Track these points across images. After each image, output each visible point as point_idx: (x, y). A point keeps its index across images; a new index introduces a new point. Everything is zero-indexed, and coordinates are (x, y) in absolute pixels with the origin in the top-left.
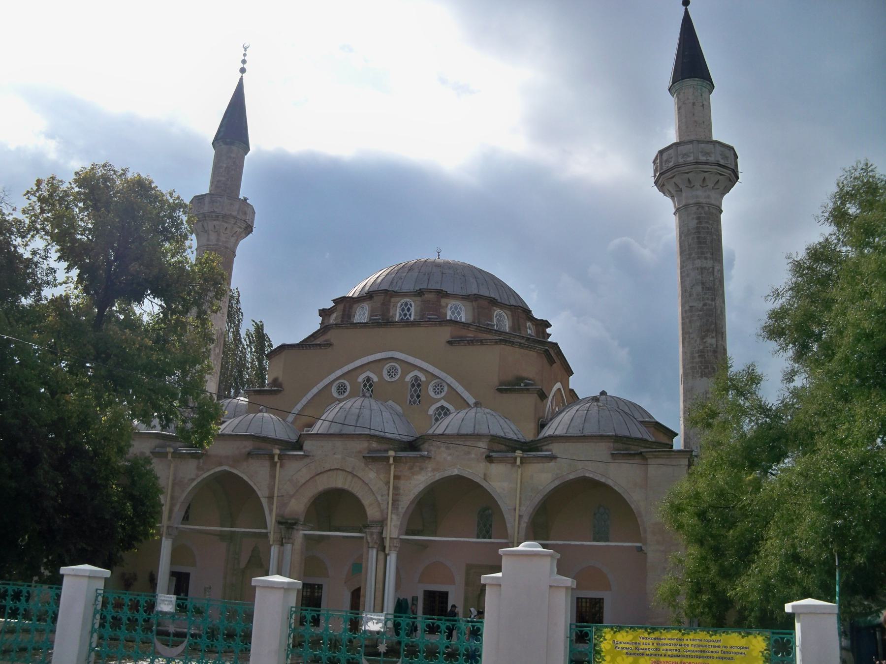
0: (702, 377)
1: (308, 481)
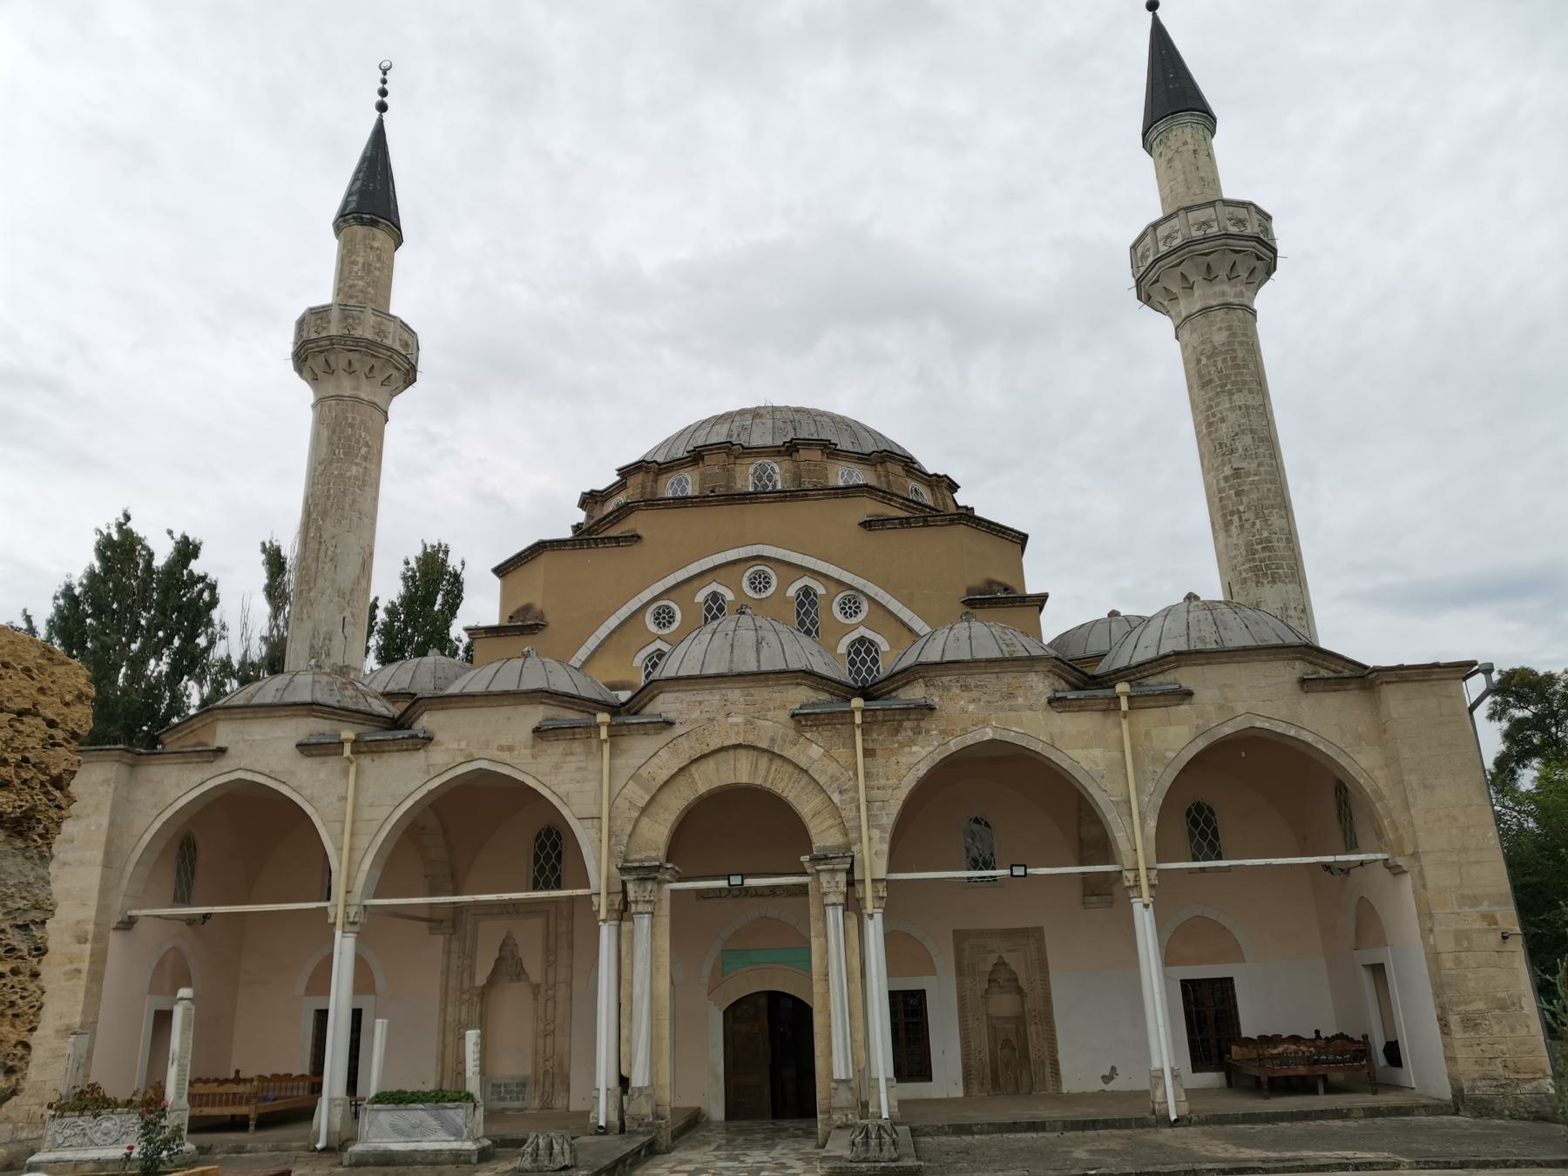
0: (1274, 581)
1: (673, 777)
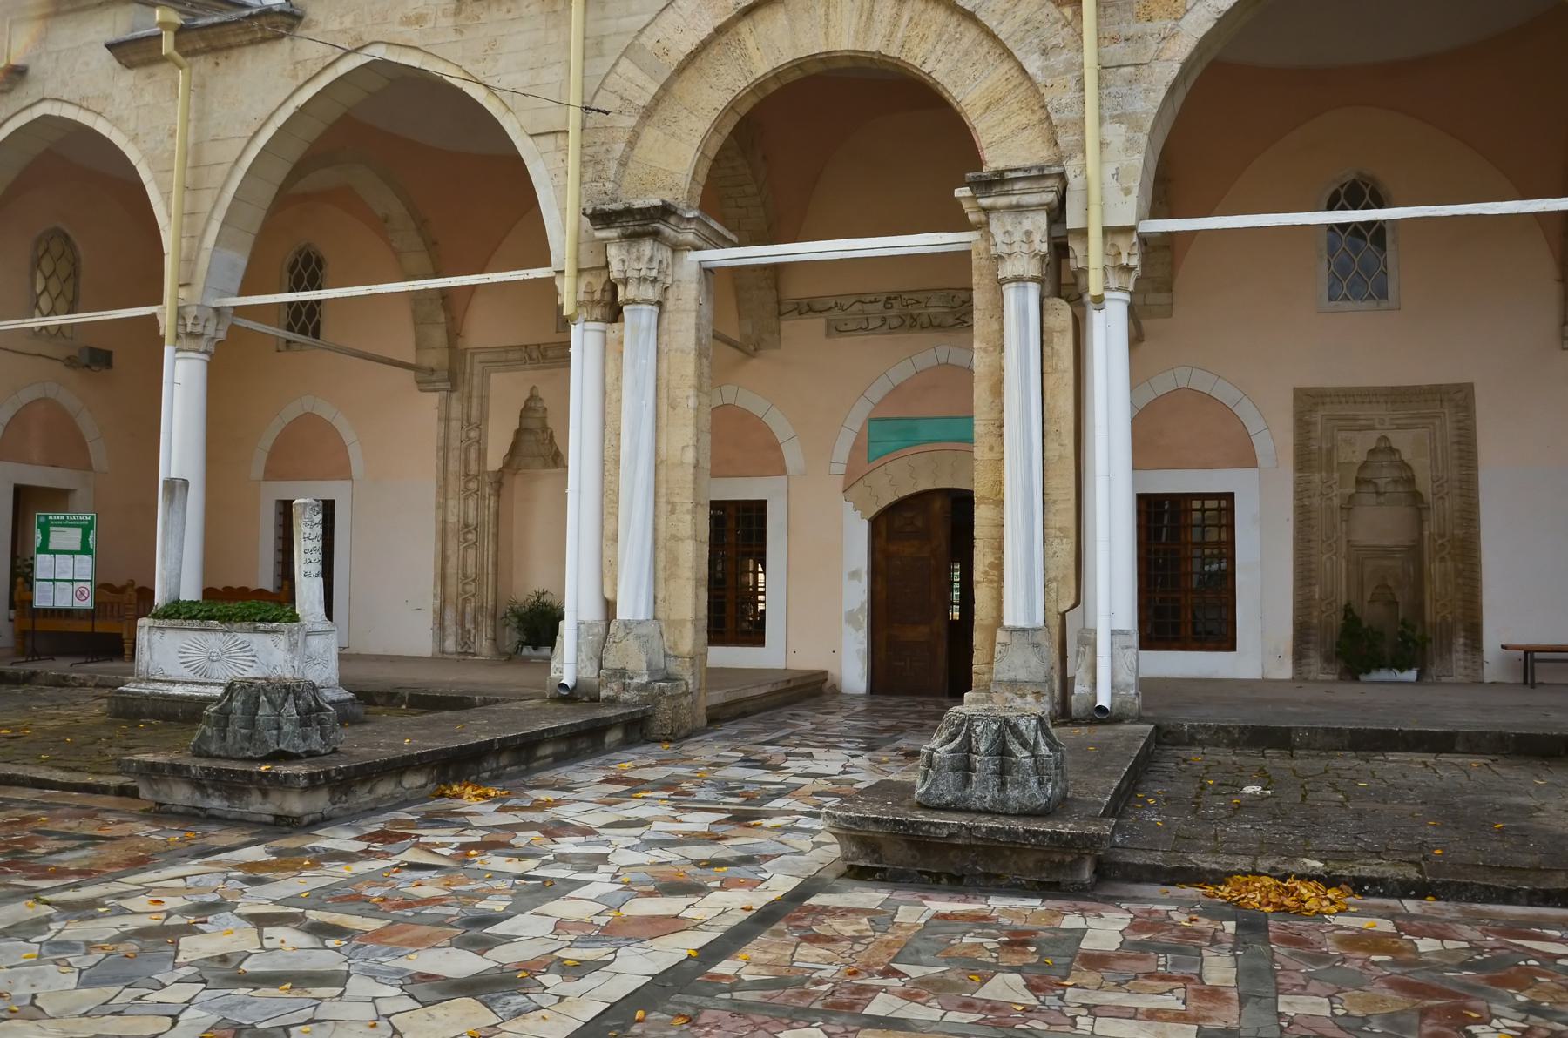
1: (704, 46)
